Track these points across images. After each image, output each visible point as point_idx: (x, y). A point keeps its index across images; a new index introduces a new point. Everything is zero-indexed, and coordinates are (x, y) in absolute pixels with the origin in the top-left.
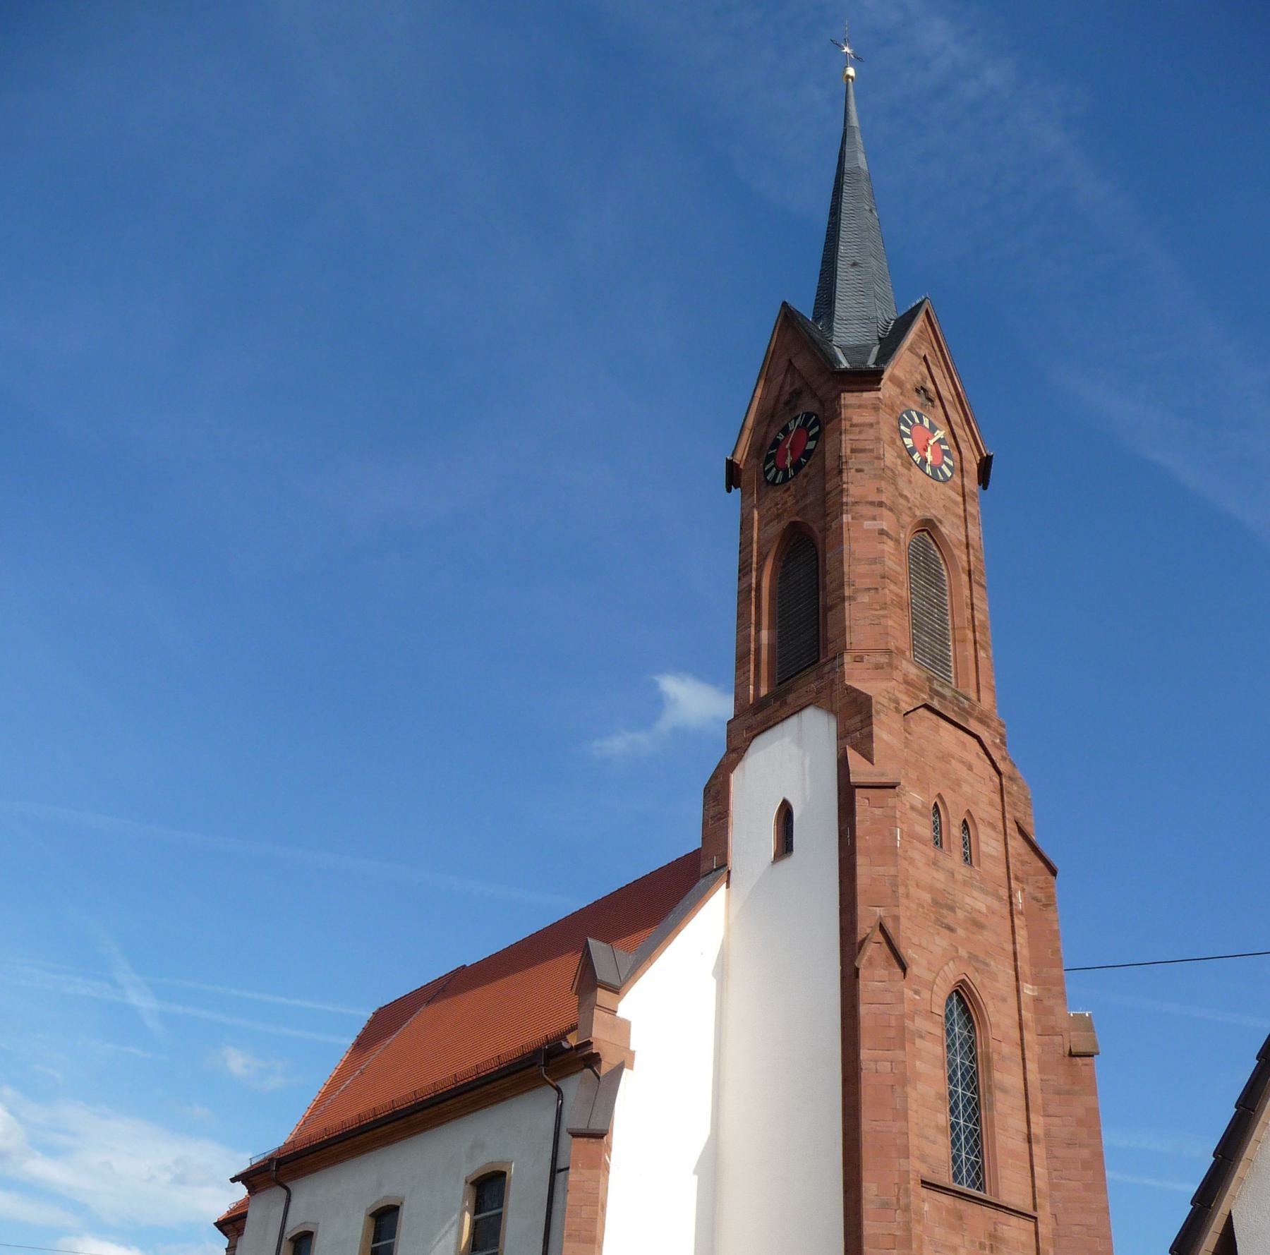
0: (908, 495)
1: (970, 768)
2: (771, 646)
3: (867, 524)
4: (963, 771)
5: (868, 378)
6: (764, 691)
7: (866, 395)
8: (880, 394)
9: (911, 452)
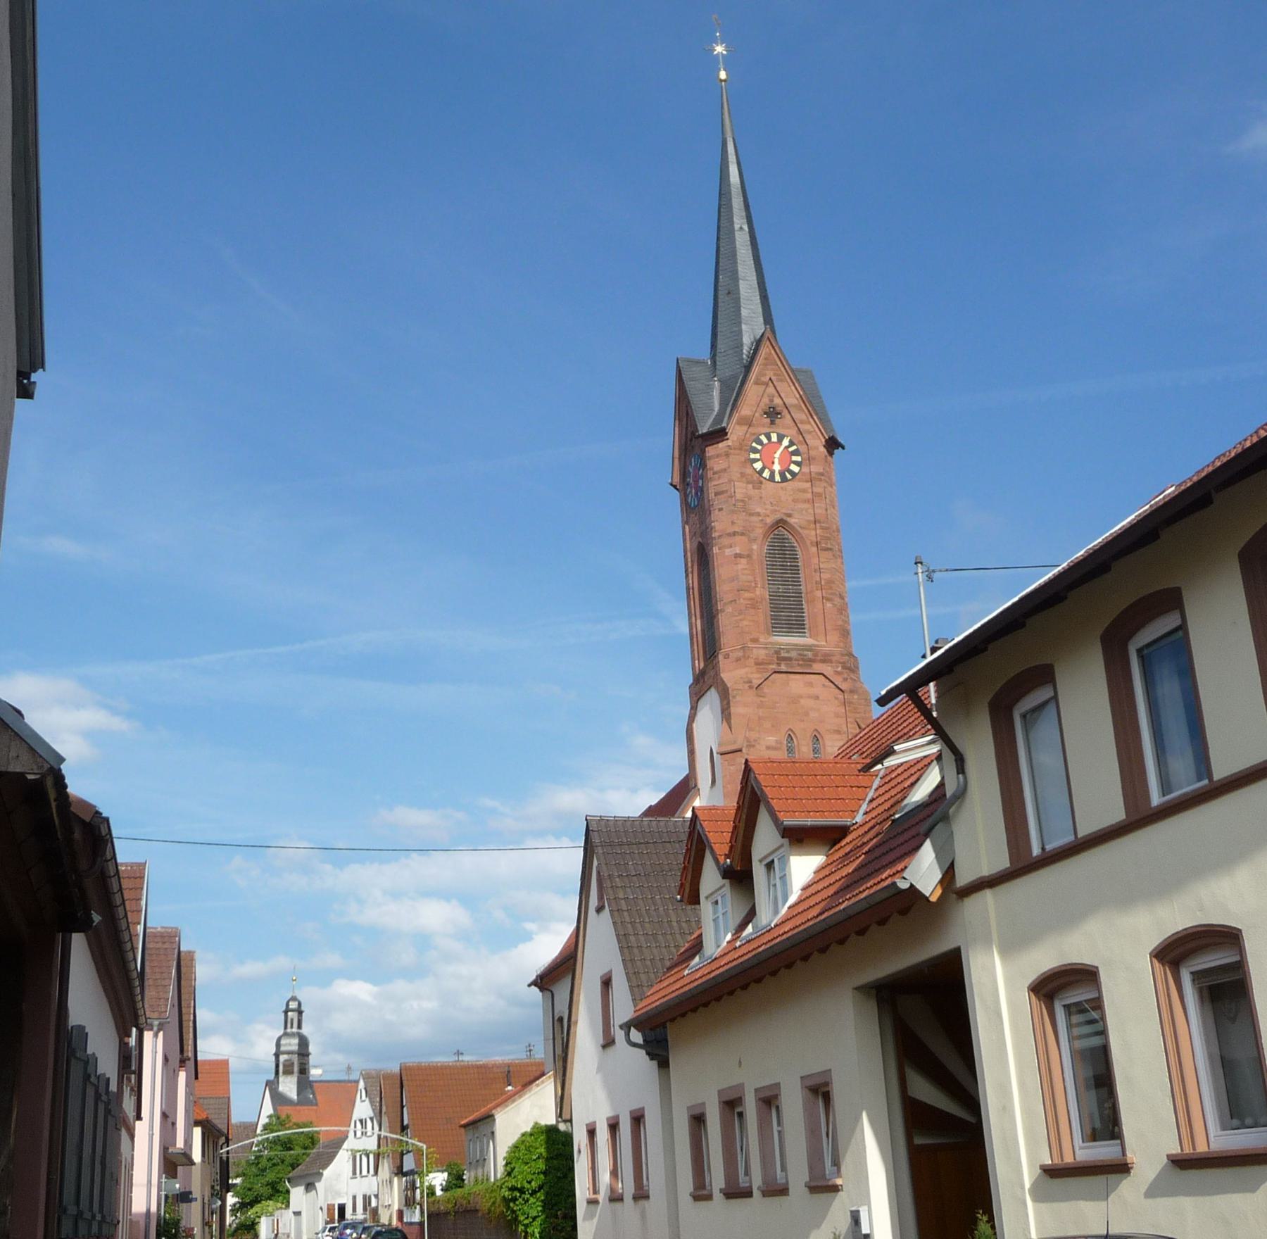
0: (758, 510)
1: (817, 698)
2: (703, 631)
3: (728, 552)
4: (809, 703)
5: (719, 434)
6: (702, 665)
7: (721, 445)
8: (729, 443)
9: (761, 472)
